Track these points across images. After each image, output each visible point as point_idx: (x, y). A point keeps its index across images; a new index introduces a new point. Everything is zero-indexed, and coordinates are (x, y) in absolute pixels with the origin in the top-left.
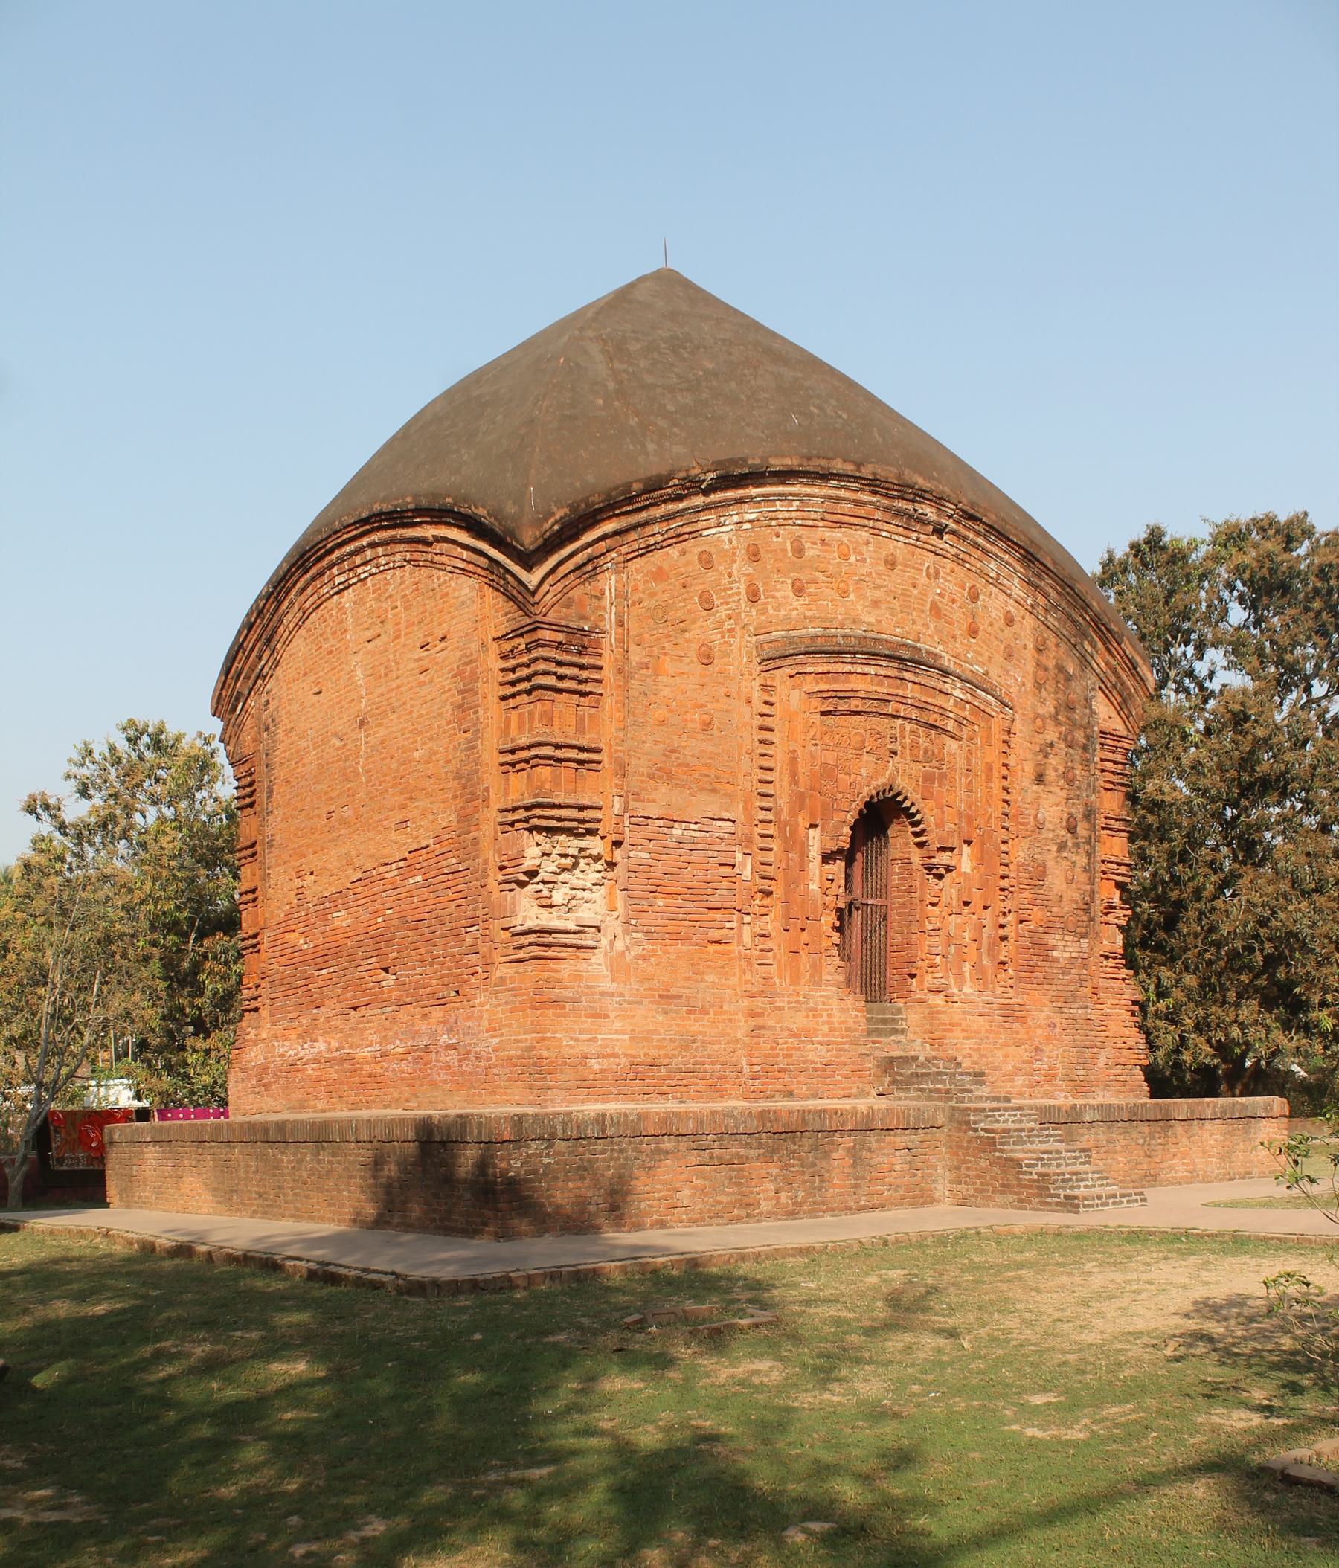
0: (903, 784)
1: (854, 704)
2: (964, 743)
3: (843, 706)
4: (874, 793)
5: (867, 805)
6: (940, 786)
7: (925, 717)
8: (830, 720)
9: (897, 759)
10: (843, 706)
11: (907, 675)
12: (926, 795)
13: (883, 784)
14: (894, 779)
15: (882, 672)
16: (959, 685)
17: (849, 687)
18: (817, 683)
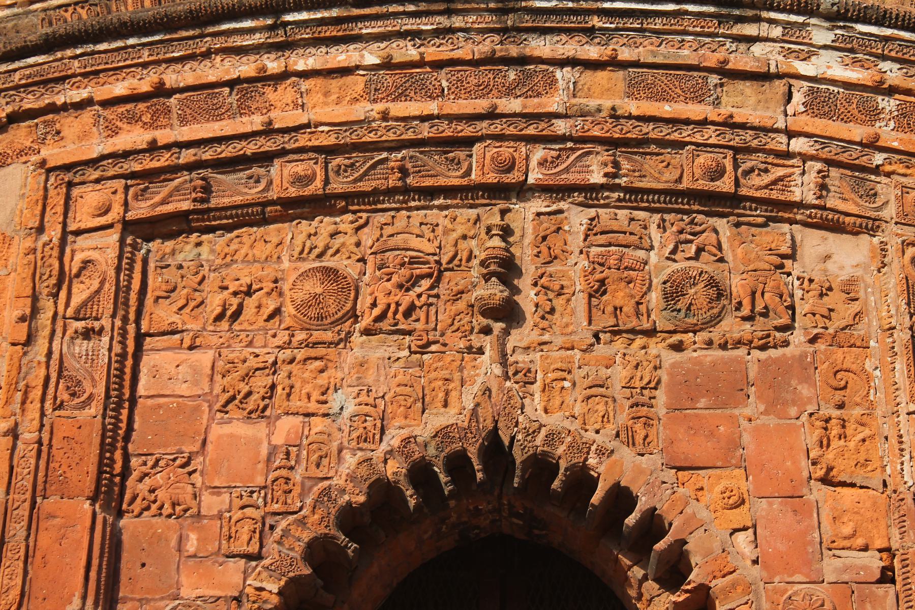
0: (555, 421)
1: (281, 178)
2: (892, 235)
3: (233, 189)
4: (394, 469)
5: (349, 519)
6: (774, 405)
7: (657, 173)
8: (186, 250)
9: (516, 338)
10: (233, 189)
11: (540, 46)
12: (693, 448)
13: (443, 434)
14: (512, 407)
15: (408, 51)
16: (821, 35)
17: (256, 122)
18: (114, 132)
